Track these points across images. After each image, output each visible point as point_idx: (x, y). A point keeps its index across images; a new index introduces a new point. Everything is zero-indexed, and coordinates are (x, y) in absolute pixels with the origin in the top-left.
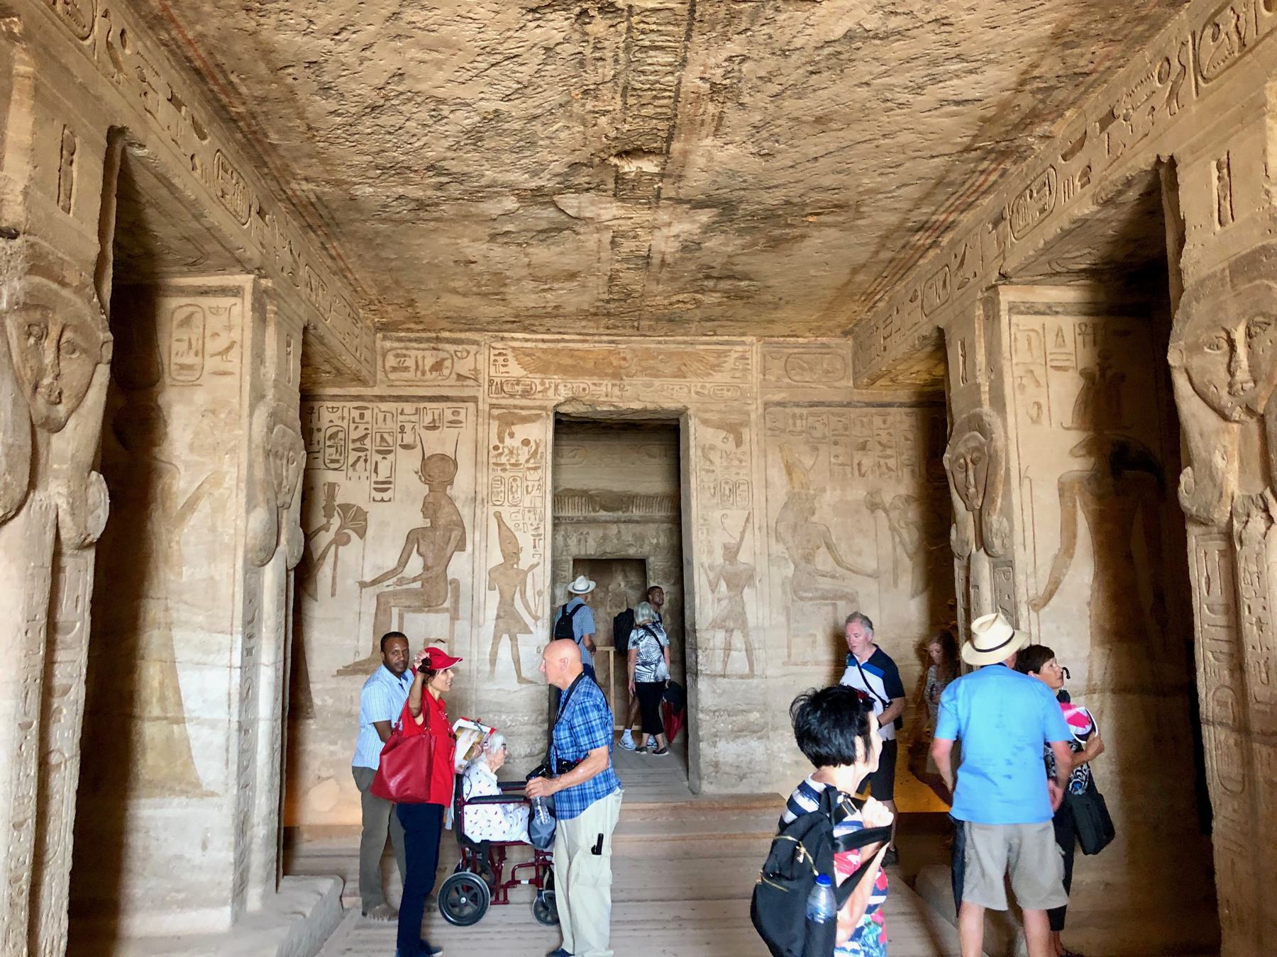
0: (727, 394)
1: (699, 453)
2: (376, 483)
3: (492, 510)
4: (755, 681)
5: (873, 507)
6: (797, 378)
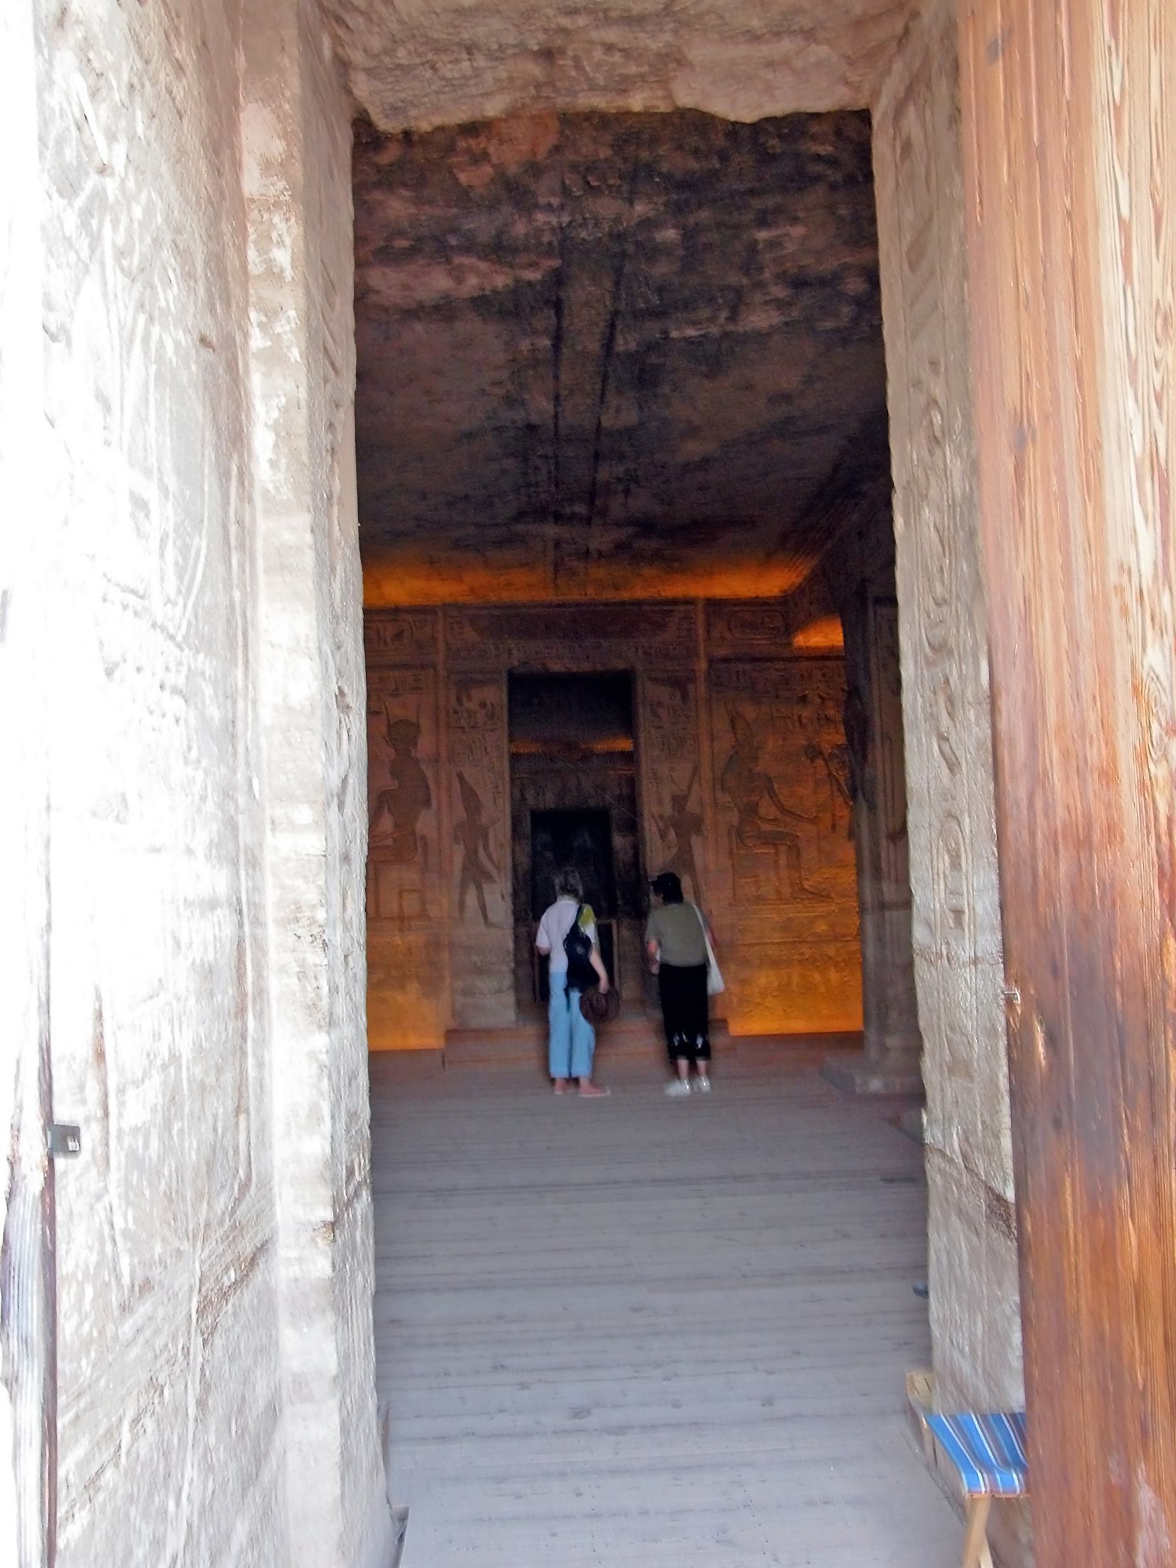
5: (814, 752)
6: (738, 636)
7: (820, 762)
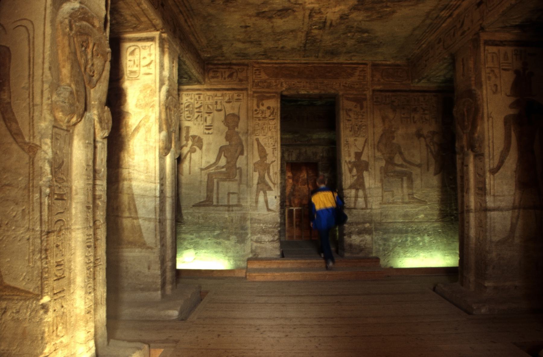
0: (356, 86)
1: (345, 113)
2: (206, 126)
3: (255, 138)
4: (368, 211)
5: (419, 135)
7: (422, 139)
